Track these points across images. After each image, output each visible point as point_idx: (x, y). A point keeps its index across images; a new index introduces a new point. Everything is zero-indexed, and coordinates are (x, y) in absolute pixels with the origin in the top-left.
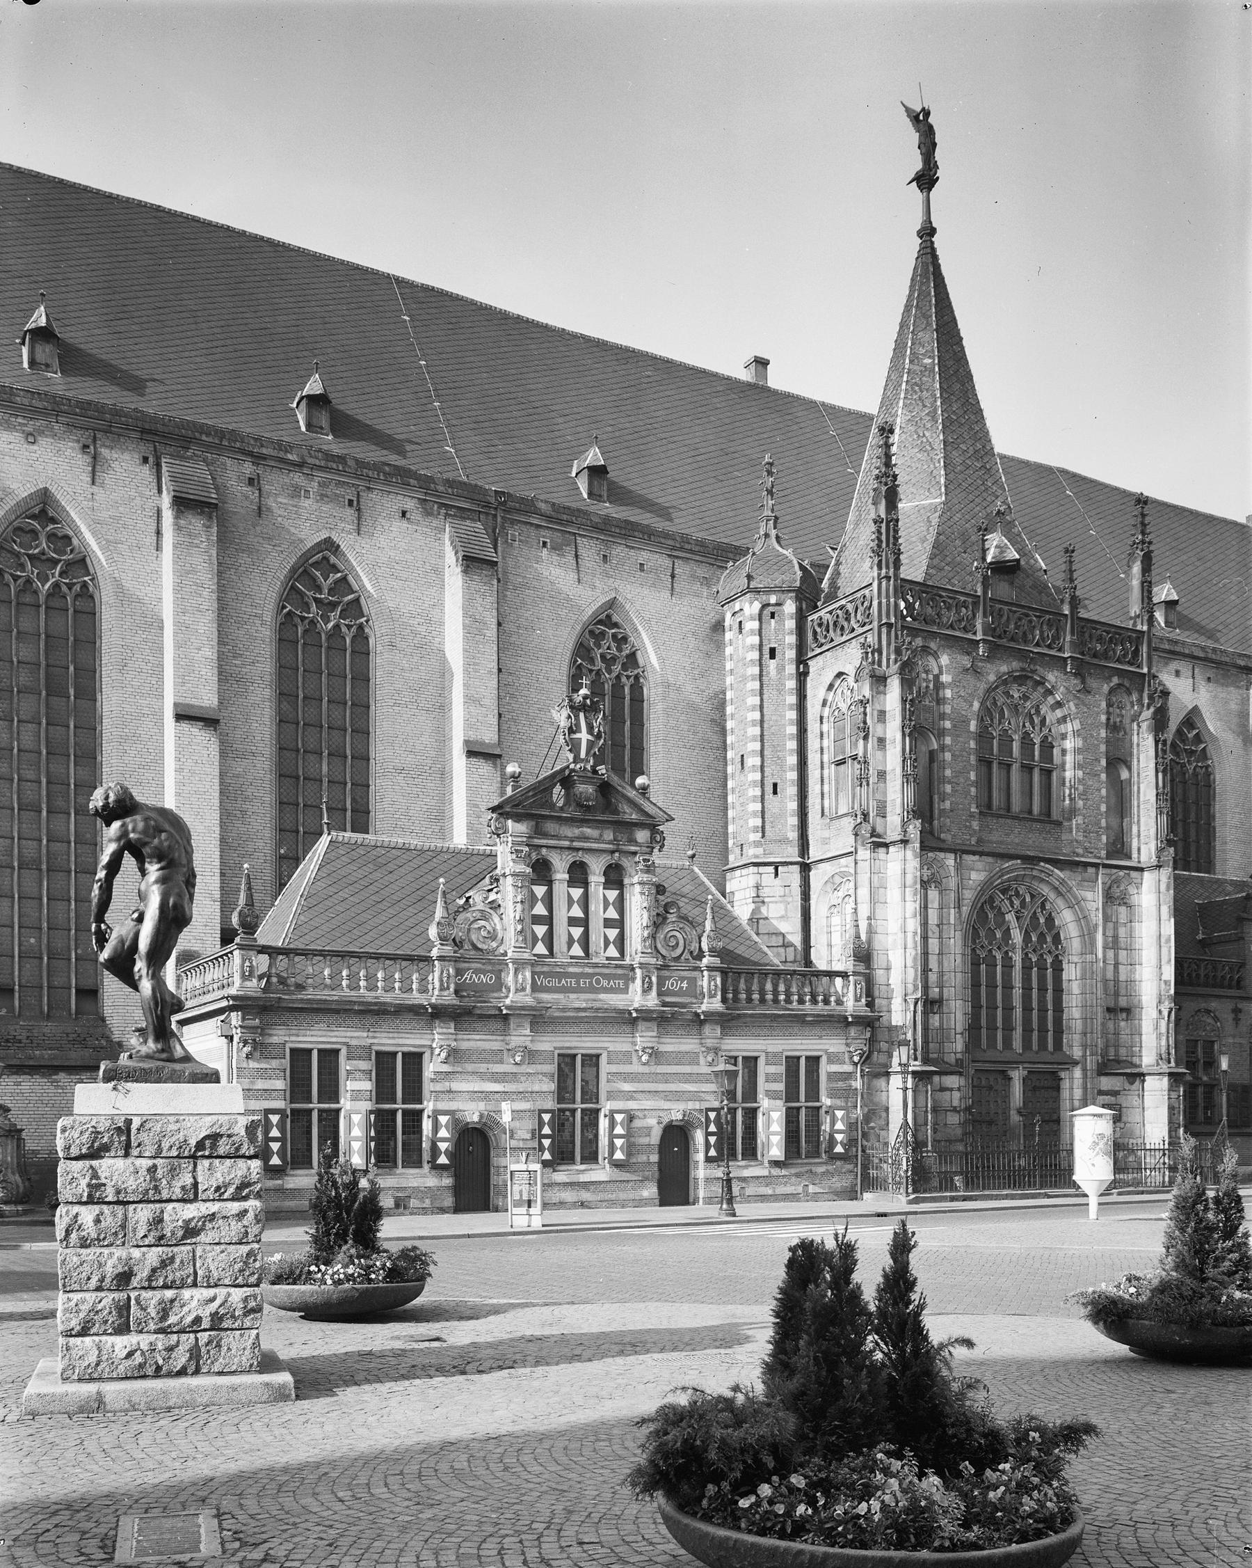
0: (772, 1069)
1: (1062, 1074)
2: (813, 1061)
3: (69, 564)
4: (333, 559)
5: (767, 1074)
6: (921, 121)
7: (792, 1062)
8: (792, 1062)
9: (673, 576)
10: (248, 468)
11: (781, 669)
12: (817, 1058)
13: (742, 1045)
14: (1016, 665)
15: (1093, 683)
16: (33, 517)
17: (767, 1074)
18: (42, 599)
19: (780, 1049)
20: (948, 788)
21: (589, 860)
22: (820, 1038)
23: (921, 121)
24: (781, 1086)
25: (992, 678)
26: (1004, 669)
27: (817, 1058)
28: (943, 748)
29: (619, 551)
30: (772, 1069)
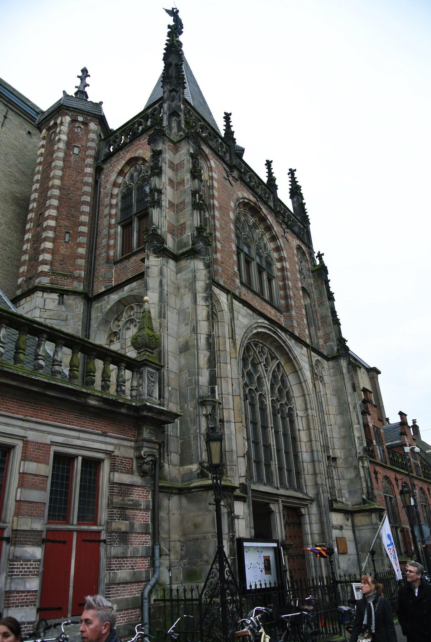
0: (32, 467)
2: (92, 465)
5: (22, 475)
6: (174, 13)
7: (63, 461)
8: (63, 461)
12: (98, 463)
17: (22, 475)
19: (48, 439)
20: (219, 245)
22: (104, 434)
23: (174, 13)
24: (42, 496)
26: (246, 195)
27: (98, 463)
28: (214, 217)
30: (32, 467)
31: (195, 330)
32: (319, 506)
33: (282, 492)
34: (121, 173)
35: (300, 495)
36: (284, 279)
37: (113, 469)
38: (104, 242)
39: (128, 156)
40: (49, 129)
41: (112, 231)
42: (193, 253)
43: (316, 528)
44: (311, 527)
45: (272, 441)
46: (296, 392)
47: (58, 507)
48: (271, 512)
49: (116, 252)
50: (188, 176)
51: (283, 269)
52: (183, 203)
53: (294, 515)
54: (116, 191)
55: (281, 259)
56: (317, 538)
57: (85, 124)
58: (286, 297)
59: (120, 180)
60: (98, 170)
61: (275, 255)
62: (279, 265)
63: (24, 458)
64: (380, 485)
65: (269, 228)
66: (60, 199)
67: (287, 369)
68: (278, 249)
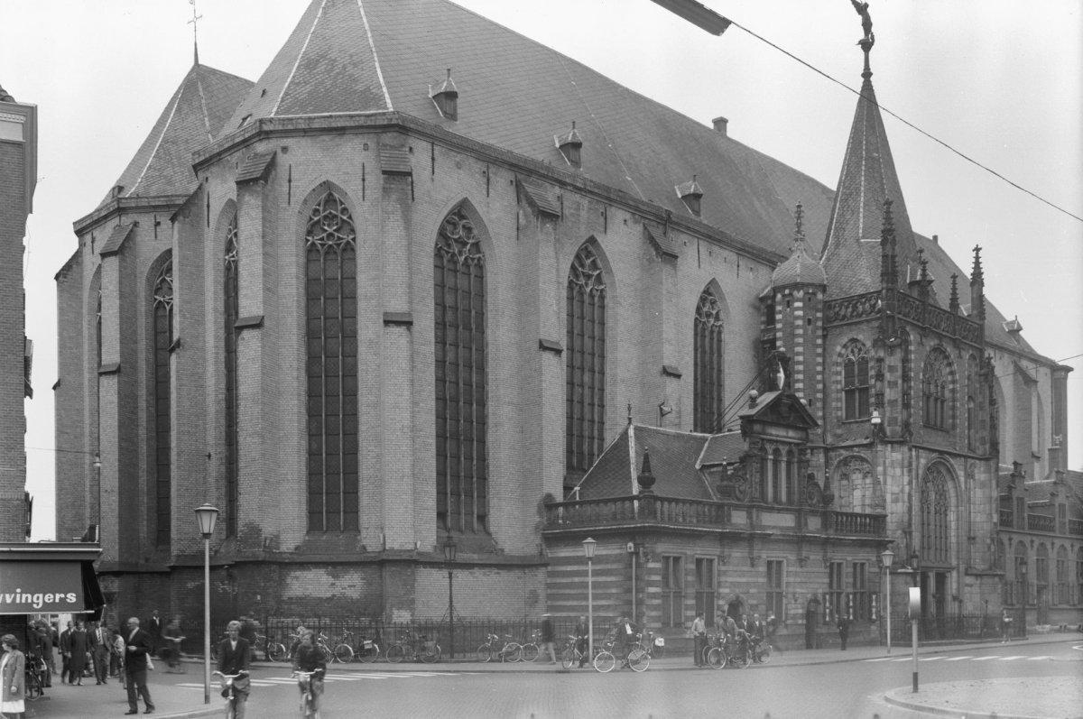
1: (948, 575)
3: (473, 245)
4: (590, 248)
7: (855, 564)
9: (738, 266)
10: (557, 190)
11: (814, 332)
13: (838, 556)
14: (936, 342)
15: (963, 353)
16: (454, 214)
18: (459, 267)
21: (781, 447)
24: (851, 580)
25: (928, 349)
26: (932, 344)
29: (716, 249)
31: (902, 491)
32: (958, 572)
33: (936, 565)
34: (845, 346)
35: (945, 565)
36: (954, 400)
37: (869, 567)
38: (834, 404)
39: (850, 336)
40: (784, 296)
41: (839, 395)
42: (901, 443)
43: (955, 586)
44: (952, 584)
45: (932, 534)
46: (952, 493)
47: (854, 585)
48: (929, 577)
49: (842, 414)
50: (900, 382)
51: (953, 391)
52: (896, 401)
53: (941, 579)
54: (839, 360)
55: (954, 382)
56: (954, 591)
57: (814, 294)
58: (954, 417)
59: (843, 351)
60: (824, 337)
61: (950, 378)
62: (951, 387)
63: (847, 567)
64: (1013, 549)
65: (947, 357)
66: (804, 372)
67: (948, 478)
68: (952, 373)
